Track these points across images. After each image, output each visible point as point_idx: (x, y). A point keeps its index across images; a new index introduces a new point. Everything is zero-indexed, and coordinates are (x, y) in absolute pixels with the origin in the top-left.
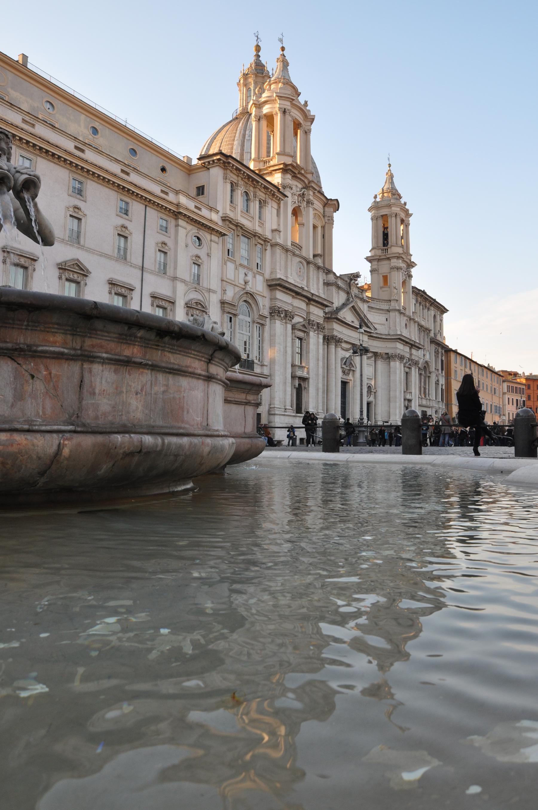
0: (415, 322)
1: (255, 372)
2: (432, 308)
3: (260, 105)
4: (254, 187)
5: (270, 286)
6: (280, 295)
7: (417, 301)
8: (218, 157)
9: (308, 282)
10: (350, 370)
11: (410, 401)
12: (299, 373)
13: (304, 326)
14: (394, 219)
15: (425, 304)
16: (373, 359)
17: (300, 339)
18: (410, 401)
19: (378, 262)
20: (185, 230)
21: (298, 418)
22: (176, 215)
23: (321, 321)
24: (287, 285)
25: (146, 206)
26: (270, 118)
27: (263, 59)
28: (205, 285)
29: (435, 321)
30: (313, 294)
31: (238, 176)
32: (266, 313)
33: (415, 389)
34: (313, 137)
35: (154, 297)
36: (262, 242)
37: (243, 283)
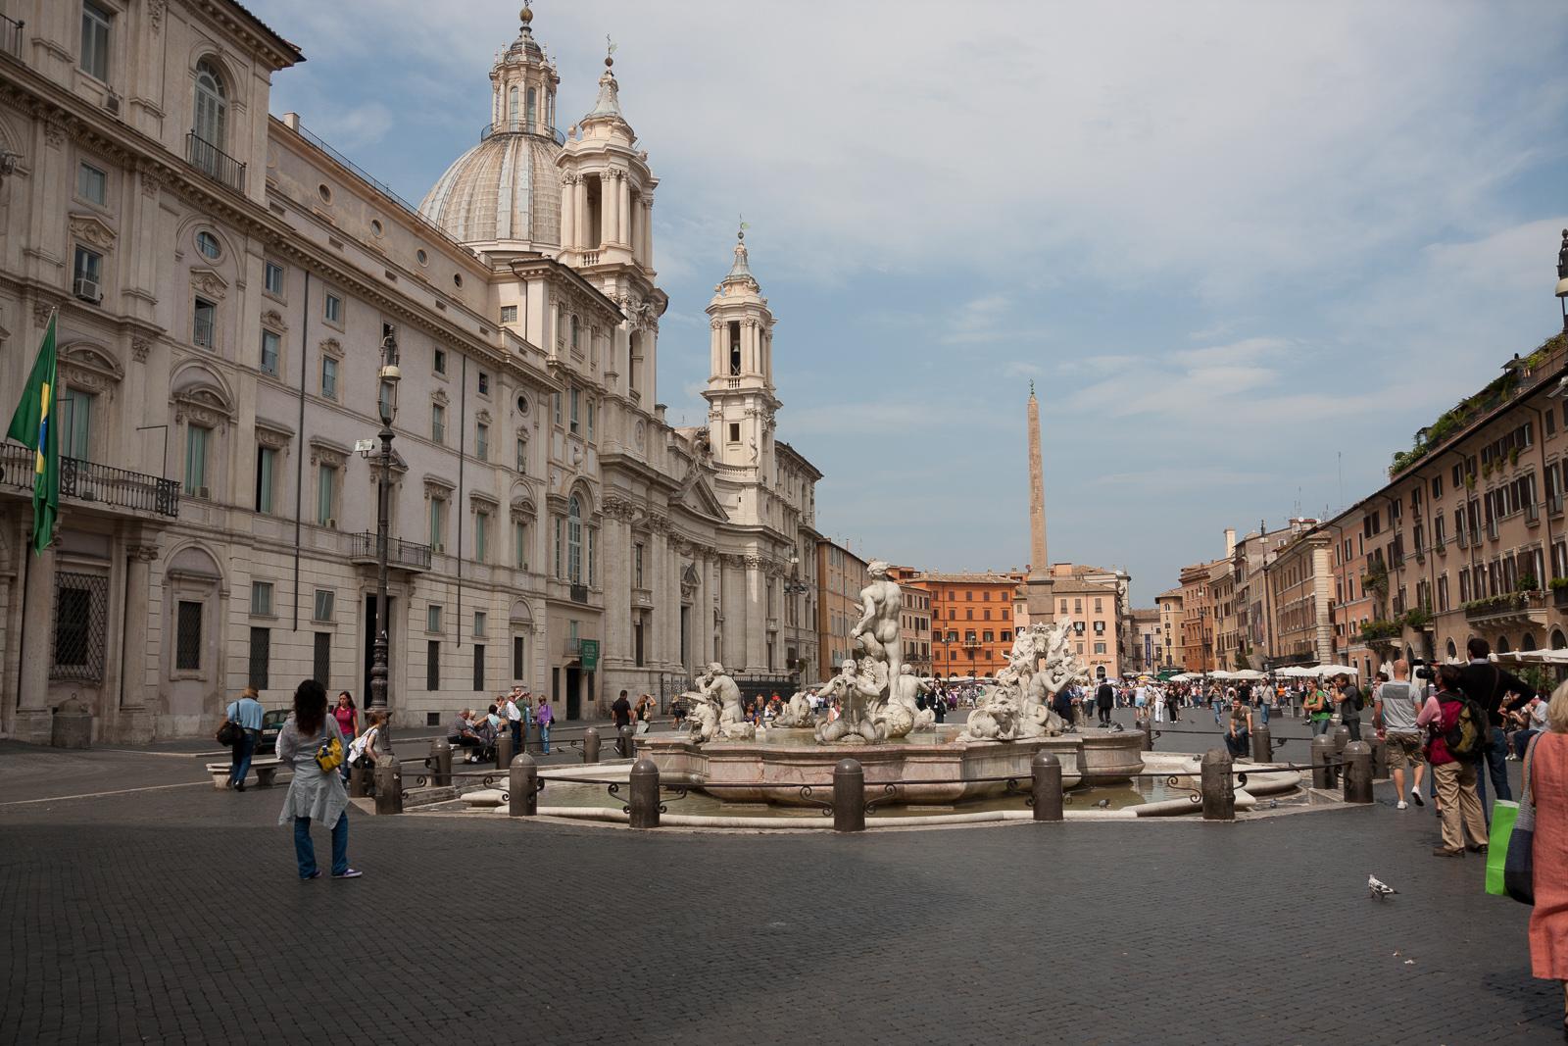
0: (779, 501)
1: (589, 604)
2: (800, 474)
3: (576, 158)
4: (585, 308)
5: (603, 465)
6: (617, 479)
7: (780, 465)
8: (547, 267)
9: (649, 451)
10: (689, 588)
11: (774, 633)
12: (642, 601)
13: (646, 526)
14: (750, 329)
15: (792, 468)
16: (719, 565)
17: (640, 546)
18: (774, 633)
19: (722, 401)
20: (510, 390)
21: (640, 674)
22: (499, 367)
23: (664, 514)
24: (629, 464)
25: (465, 356)
26: (593, 185)
27: (538, 37)
28: (532, 474)
29: (804, 496)
30: (658, 474)
31: (567, 293)
32: (598, 508)
33: (780, 613)
34: (655, 211)
35: (475, 499)
36: (594, 396)
37: (573, 464)
